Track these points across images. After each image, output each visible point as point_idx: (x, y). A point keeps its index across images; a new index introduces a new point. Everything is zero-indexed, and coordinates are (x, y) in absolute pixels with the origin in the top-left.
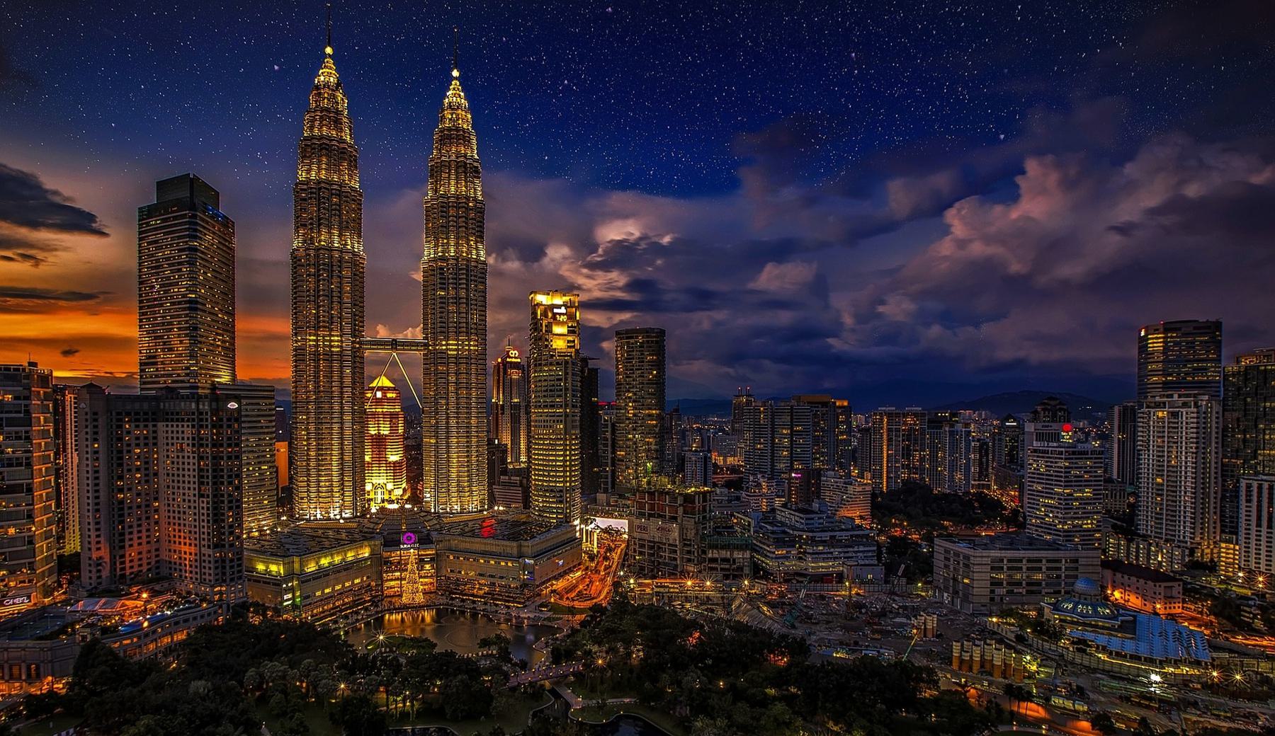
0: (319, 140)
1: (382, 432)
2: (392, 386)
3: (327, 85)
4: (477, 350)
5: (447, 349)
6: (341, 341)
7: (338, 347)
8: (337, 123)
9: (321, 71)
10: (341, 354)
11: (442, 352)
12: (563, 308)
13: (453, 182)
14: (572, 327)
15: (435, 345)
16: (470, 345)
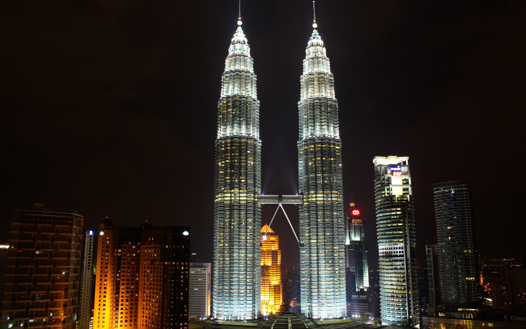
0: (234, 72)
1: (266, 264)
2: (274, 232)
3: (239, 42)
4: (337, 201)
5: (316, 201)
6: (247, 197)
7: (244, 200)
8: (245, 61)
9: (235, 34)
10: (246, 206)
11: (312, 202)
12: (399, 166)
13: (316, 90)
14: (405, 180)
15: (309, 198)
16: (332, 197)
